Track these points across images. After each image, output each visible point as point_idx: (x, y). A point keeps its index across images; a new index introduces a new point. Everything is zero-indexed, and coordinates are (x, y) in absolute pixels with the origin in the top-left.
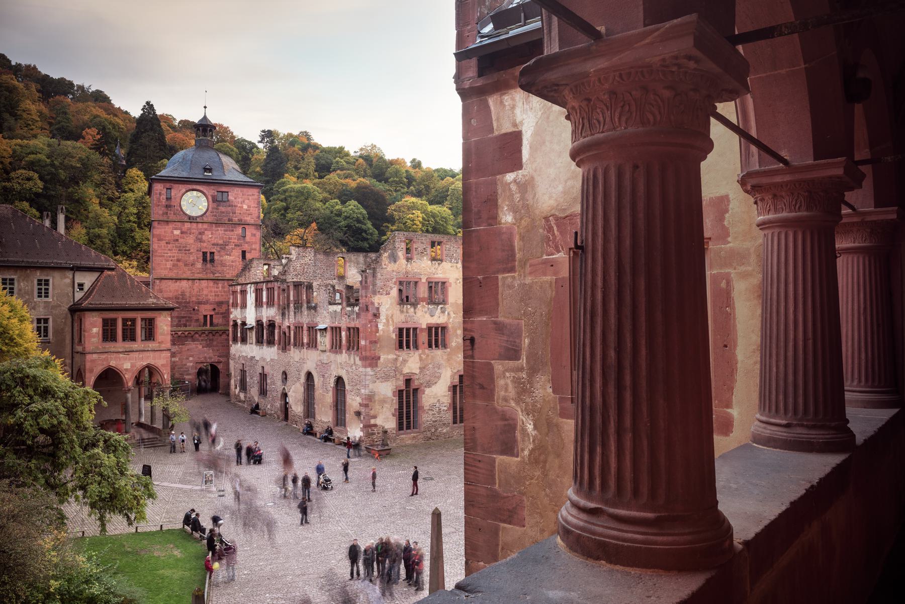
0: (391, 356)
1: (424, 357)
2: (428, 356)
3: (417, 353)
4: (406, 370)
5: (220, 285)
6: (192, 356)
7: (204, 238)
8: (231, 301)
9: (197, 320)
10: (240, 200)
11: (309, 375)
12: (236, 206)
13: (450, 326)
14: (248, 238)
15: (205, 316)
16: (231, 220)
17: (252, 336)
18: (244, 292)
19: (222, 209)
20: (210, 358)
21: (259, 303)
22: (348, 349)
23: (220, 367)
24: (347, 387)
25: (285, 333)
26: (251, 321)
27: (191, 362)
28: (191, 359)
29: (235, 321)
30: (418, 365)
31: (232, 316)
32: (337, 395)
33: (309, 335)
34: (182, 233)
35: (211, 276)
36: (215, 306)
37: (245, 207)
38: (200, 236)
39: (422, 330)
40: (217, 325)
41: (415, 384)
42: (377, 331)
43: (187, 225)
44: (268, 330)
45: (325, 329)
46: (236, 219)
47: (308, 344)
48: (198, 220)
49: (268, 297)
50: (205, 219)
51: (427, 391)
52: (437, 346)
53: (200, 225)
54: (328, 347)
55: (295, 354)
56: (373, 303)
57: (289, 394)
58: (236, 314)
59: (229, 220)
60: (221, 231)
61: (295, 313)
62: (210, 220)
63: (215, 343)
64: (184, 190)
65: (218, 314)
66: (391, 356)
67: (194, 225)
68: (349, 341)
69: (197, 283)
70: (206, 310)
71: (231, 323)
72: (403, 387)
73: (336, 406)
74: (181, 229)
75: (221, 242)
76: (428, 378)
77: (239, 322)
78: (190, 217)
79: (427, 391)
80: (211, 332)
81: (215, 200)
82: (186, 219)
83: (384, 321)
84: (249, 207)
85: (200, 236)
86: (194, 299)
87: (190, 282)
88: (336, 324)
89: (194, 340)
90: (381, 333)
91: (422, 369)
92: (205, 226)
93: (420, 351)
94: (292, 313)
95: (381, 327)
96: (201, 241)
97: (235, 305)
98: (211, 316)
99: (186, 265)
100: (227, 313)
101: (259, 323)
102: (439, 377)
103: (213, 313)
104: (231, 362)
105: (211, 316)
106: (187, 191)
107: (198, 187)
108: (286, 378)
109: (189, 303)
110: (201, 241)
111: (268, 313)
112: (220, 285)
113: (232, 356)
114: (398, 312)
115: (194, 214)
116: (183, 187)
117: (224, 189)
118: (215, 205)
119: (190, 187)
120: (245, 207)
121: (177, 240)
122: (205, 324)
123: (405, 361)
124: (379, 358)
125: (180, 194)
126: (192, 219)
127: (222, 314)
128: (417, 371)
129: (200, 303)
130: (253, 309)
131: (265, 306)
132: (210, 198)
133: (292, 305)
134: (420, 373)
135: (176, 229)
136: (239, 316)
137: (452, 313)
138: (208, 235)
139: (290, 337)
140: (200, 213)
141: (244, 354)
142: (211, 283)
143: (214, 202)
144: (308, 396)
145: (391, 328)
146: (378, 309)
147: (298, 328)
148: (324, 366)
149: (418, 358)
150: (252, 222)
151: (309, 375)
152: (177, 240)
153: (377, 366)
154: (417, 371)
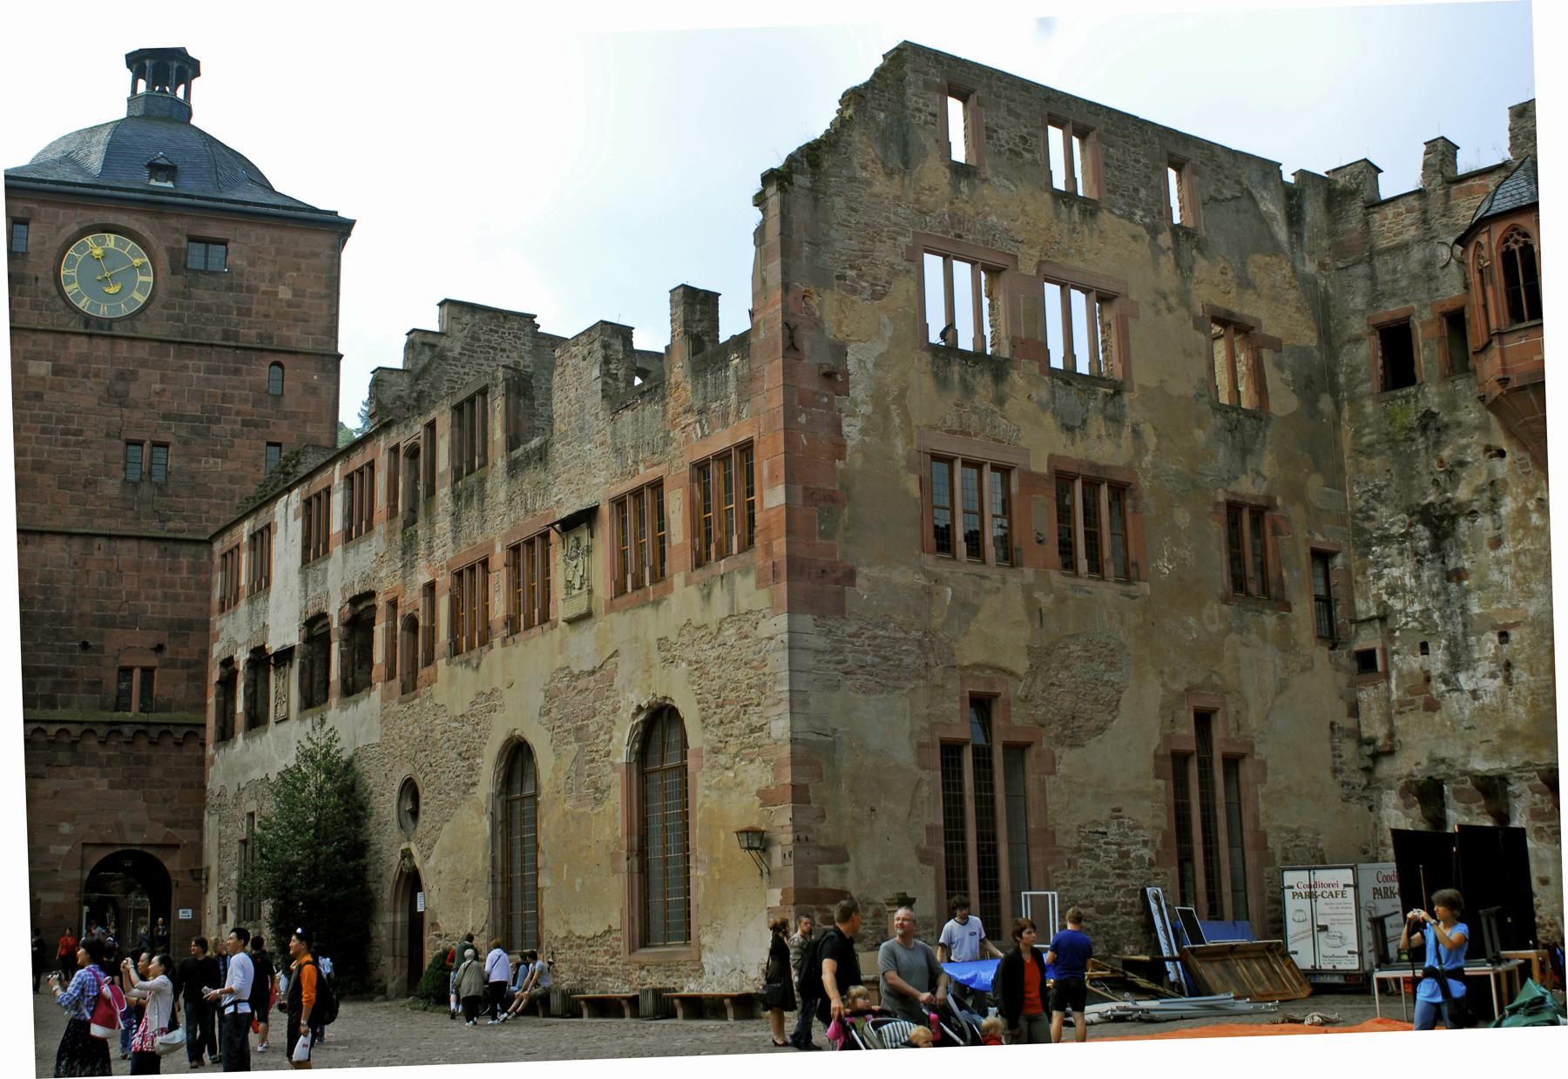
0: (905, 577)
1: (1045, 600)
2: (1061, 600)
3: (1015, 579)
4: (971, 652)
5: (184, 561)
6: (70, 818)
7: (135, 391)
8: (217, 594)
9: (95, 686)
10: (267, 270)
11: (517, 755)
12: (250, 289)
13: (1144, 484)
14: (289, 403)
15: (126, 672)
16: (236, 336)
17: (286, 687)
18: (262, 538)
19: (203, 295)
20: (140, 829)
21: (314, 548)
22: (700, 561)
23: (172, 863)
24: (694, 741)
25: (412, 623)
26: (284, 632)
27: (65, 839)
28: (65, 828)
29: (228, 663)
30: (1023, 635)
31: (217, 651)
32: (644, 799)
33: (515, 584)
34: (56, 371)
35: (153, 528)
36: (164, 637)
37: (285, 293)
38: (120, 387)
39: (1030, 478)
40: (166, 707)
41: (1011, 722)
42: (839, 449)
43: (77, 346)
44: (346, 641)
45: (587, 517)
46: (249, 335)
47: (512, 625)
48: (117, 330)
49: (349, 516)
50: (142, 329)
51: (1067, 759)
52: (1096, 567)
53: (123, 348)
54: (602, 586)
55: (450, 685)
56: (817, 324)
57: (427, 879)
58: (232, 637)
59: (226, 335)
60: (195, 369)
61: (456, 517)
62: (158, 333)
63: (156, 773)
64: (74, 228)
65: (171, 664)
66: (905, 577)
67: (103, 346)
68: (702, 530)
69: (100, 549)
70: (130, 647)
71: (215, 675)
72: (962, 728)
73: (641, 850)
74: (55, 359)
75: (193, 409)
76: (1068, 702)
77: (242, 657)
78: (88, 320)
79: (1067, 759)
80: (142, 730)
81: (178, 264)
82: (75, 325)
83: (866, 409)
84: (297, 293)
85: (120, 387)
86: (87, 608)
87: (77, 545)
88: (645, 475)
89: (79, 761)
90: (854, 460)
91: (1041, 657)
92: (142, 351)
93: (1029, 573)
94: (444, 524)
95: (852, 430)
96: (122, 400)
97: (229, 602)
98: (148, 672)
99: (64, 484)
100: (201, 628)
101: (315, 625)
102: (1114, 706)
103: (152, 661)
104: (210, 822)
105: (148, 672)
106: (85, 232)
107: (123, 220)
108: (415, 814)
109: (68, 619)
110: (122, 400)
111: (344, 572)
112: (184, 561)
113: (211, 800)
114: (928, 382)
115: (103, 312)
116: (72, 220)
117: (213, 230)
118: (178, 282)
119: (98, 217)
120: (285, 293)
121: (39, 396)
122: (122, 703)
123: (966, 609)
124: (850, 576)
125: (59, 242)
126: (95, 329)
127: (187, 665)
128: (1021, 665)
129: (107, 622)
130: (295, 579)
131: (337, 550)
132: (164, 259)
133: (443, 492)
134: (1034, 671)
135: (37, 357)
136: (241, 638)
137: (1147, 429)
138: (149, 383)
139: (431, 632)
140: (125, 310)
141: (256, 774)
142: (152, 554)
143: (175, 270)
144: (508, 855)
145: (900, 447)
146: (840, 350)
147: (471, 575)
148: (574, 692)
149: (1018, 600)
150: (309, 346)
151: (517, 755)
152: (39, 396)
153: (840, 610)
154: (1021, 665)
